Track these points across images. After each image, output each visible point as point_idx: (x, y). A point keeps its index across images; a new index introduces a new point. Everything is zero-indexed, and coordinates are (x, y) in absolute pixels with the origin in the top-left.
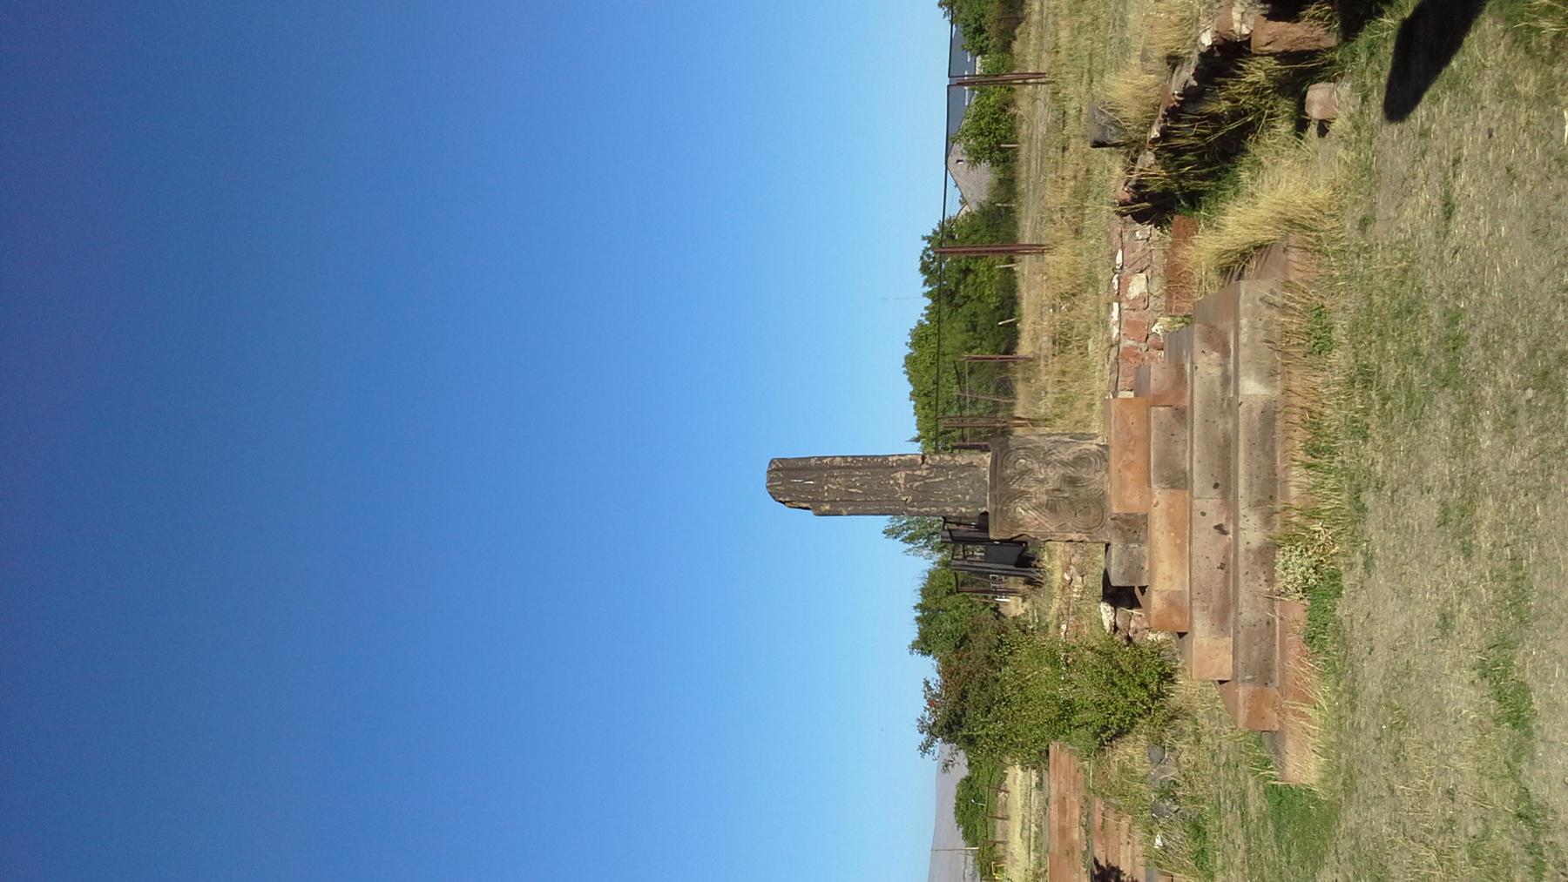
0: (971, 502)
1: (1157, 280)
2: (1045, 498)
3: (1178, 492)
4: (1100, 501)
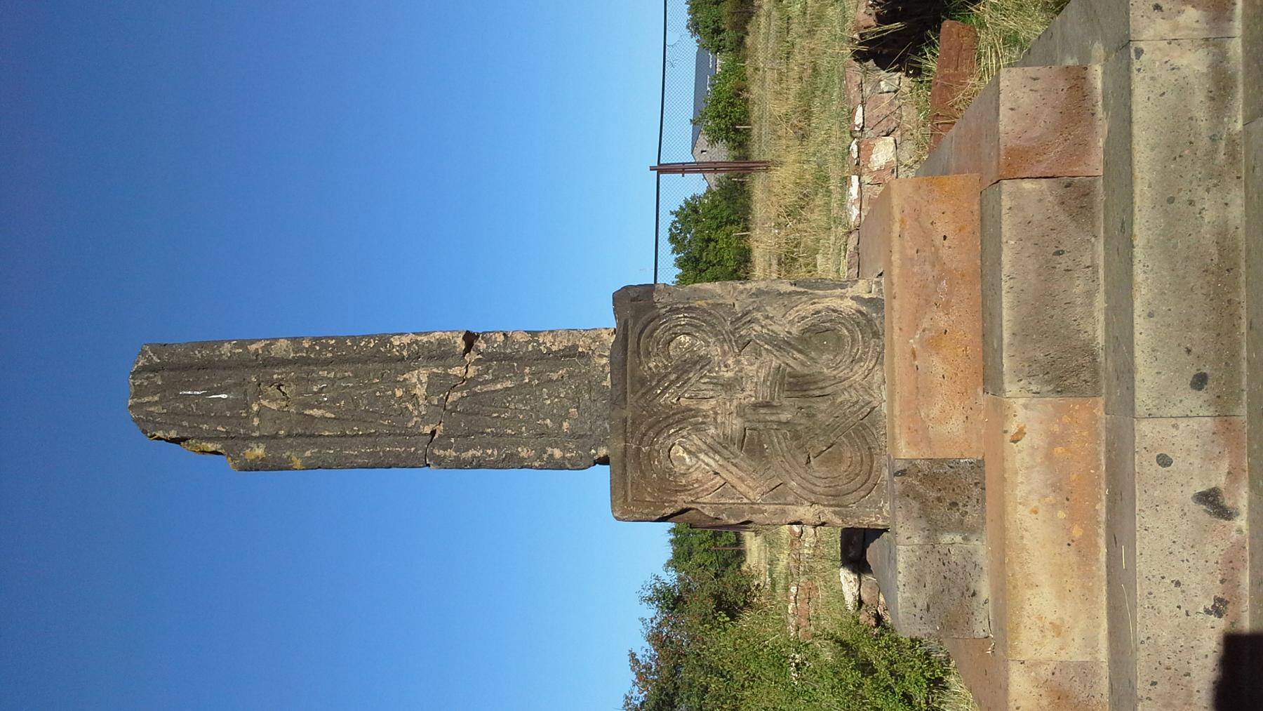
0: (573, 435)
1: (909, 147)
2: (736, 424)
3: (1073, 403)
4: (863, 429)
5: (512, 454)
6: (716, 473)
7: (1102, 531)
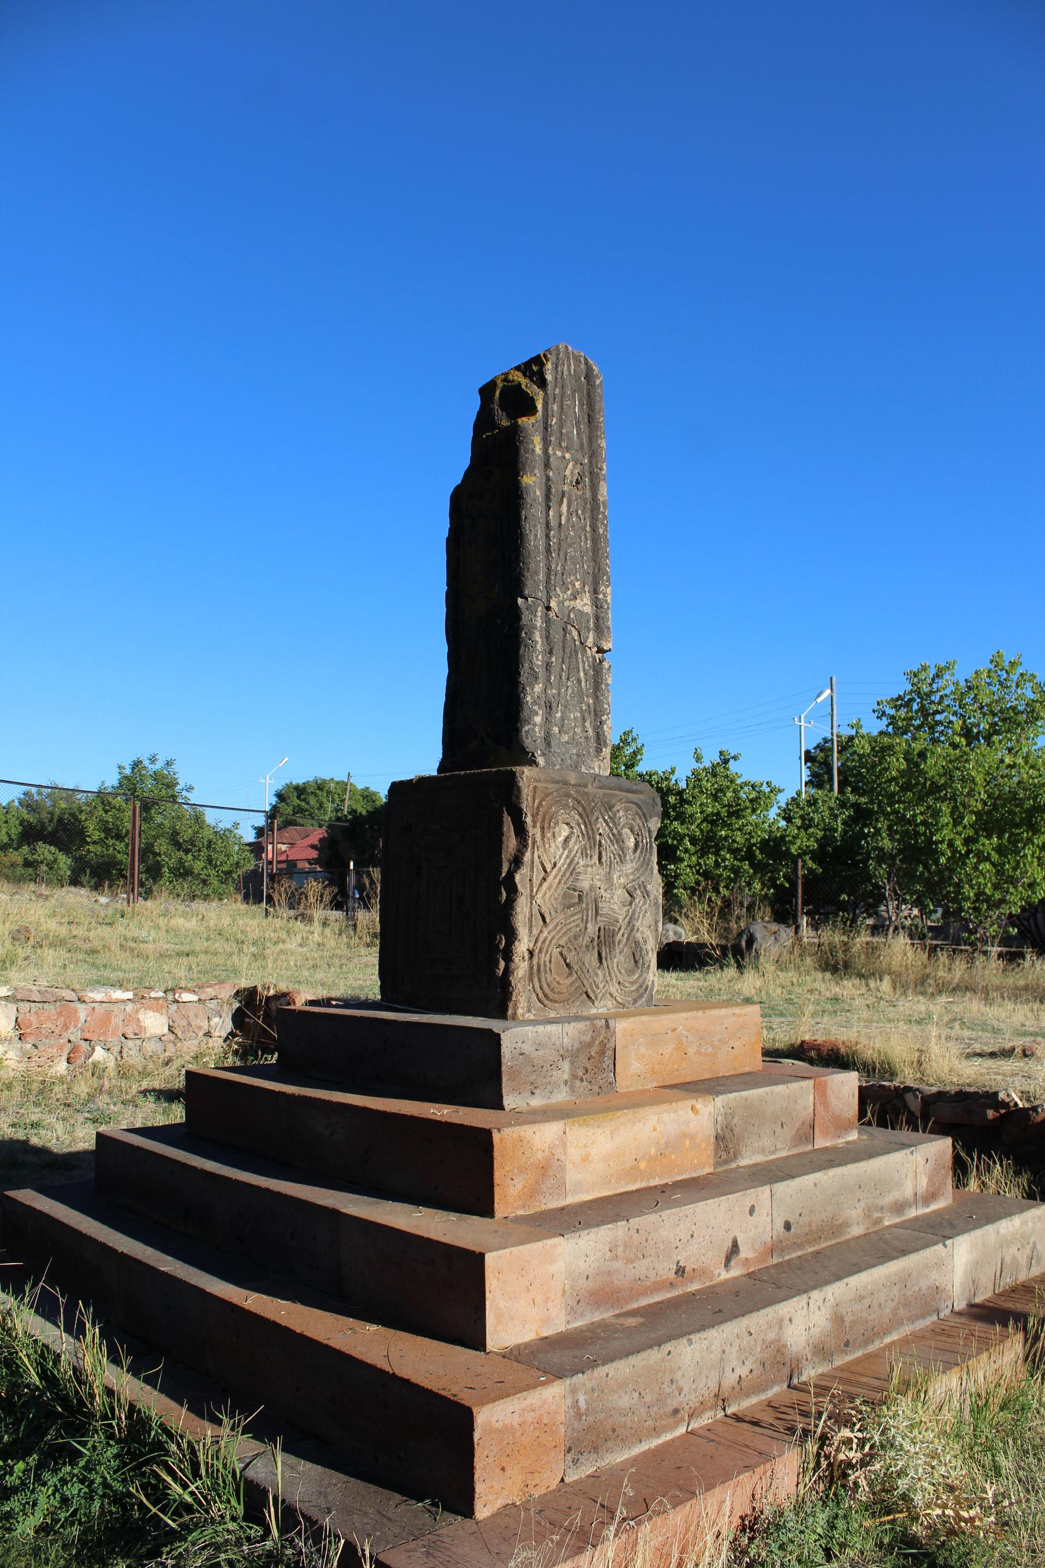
1: (158, 1047)
3: (711, 1150)
5: (537, 678)
6: (555, 865)
7: (644, 1184)
